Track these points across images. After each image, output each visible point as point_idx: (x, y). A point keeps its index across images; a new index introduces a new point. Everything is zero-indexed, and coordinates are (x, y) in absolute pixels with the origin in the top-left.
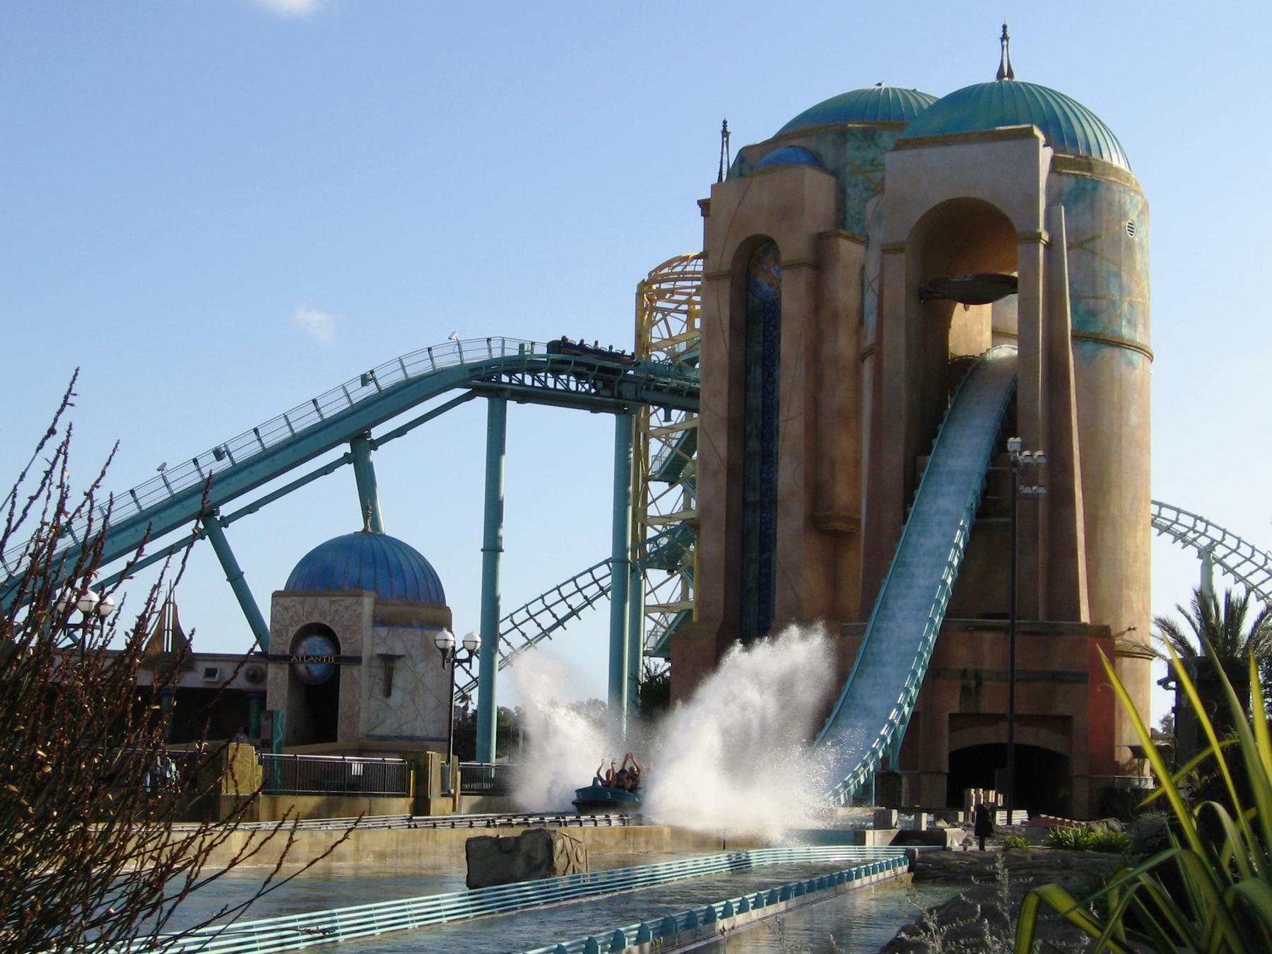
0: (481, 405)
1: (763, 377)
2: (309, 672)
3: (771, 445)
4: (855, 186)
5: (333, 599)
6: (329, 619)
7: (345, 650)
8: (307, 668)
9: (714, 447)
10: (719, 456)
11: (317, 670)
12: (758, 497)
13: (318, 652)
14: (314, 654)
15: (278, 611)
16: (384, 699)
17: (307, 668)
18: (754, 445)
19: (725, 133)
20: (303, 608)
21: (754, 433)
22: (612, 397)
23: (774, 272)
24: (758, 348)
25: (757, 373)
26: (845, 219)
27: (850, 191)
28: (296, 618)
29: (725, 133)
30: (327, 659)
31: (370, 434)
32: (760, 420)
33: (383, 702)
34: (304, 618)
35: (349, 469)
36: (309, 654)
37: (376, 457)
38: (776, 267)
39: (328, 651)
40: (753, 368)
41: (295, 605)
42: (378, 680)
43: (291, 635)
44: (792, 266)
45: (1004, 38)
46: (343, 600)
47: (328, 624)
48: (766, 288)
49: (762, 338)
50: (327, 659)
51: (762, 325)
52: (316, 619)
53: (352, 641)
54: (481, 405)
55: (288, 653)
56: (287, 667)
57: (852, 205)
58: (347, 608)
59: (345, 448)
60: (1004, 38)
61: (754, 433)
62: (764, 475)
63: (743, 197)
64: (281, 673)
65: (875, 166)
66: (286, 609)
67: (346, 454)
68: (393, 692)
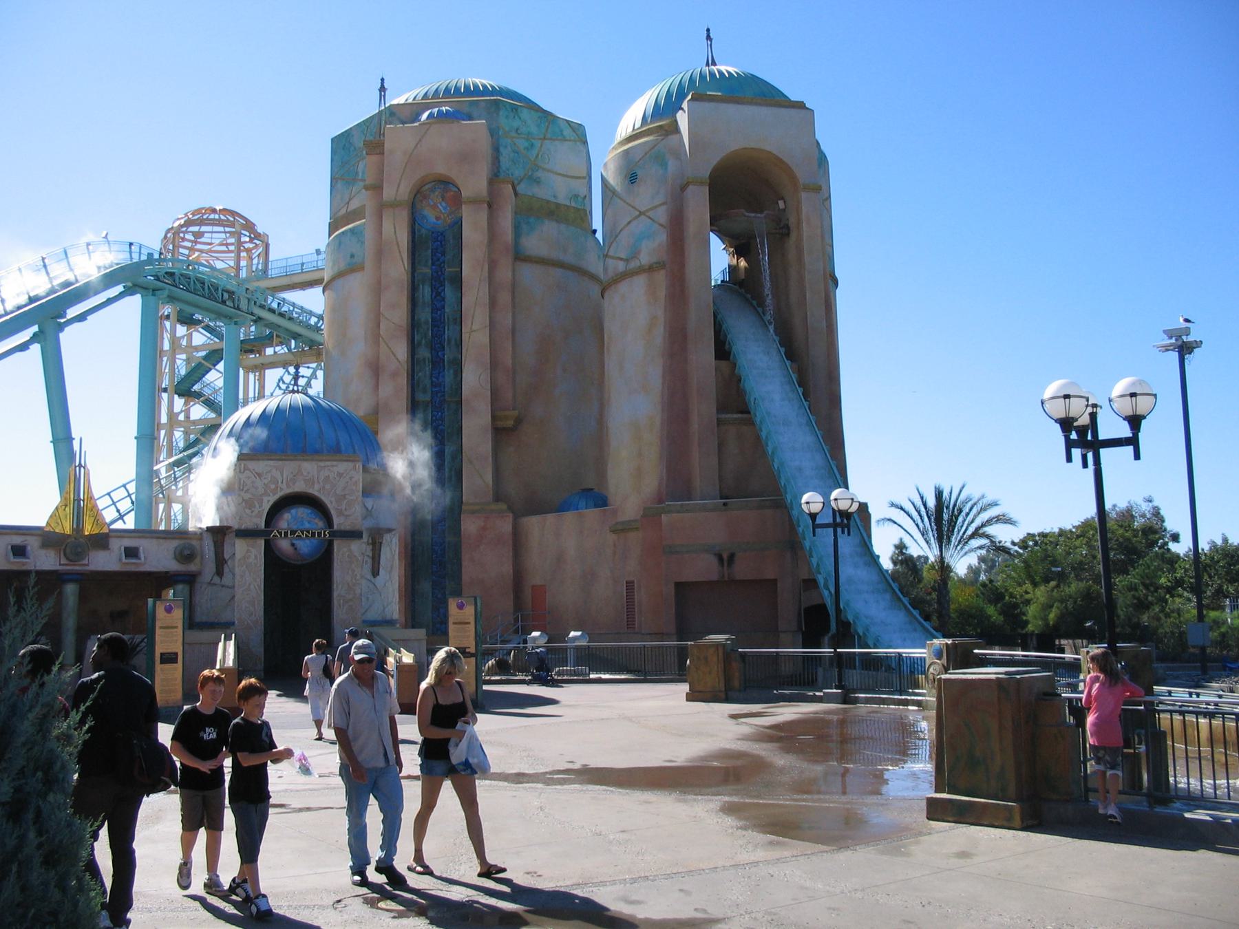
0: (135, 301)
1: (432, 295)
2: (296, 549)
3: (440, 354)
4: (506, 147)
5: (322, 464)
6: (317, 487)
7: (338, 523)
8: (293, 545)
9: (393, 353)
10: (397, 359)
11: (305, 546)
12: (428, 397)
13: (307, 526)
14: (301, 527)
15: (249, 478)
16: (373, 580)
17: (293, 545)
18: (424, 353)
19: (382, 89)
20: (282, 476)
21: (423, 342)
22: (234, 308)
23: (440, 207)
24: (426, 270)
25: (426, 292)
26: (499, 172)
27: (502, 149)
28: (273, 486)
29: (382, 89)
30: (319, 534)
31: (65, 312)
32: (430, 332)
33: (370, 581)
34: (284, 486)
35: (36, 349)
36: (295, 528)
37: (70, 338)
38: (444, 204)
39: (319, 524)
40: (421, 286)
41: (270, 471)
42: (366, 559)
43: (266, 507)
44: (474, 201)
45: (709, 37)
46: (336, 466)
47: (316, 493)
48: (432, 219)
49: (430, 262)
50: (319, 534)
51: (430, 251)
52: (299, 487)
53: (346, 513)
54: (135, 301)
55: (263, 526)
56: (262, 542)
57: (505, 162)
58: (340, 475)
59: (35, 328)
60: (709, 37)
61: (423, 342)
62: (434, 379)
63: (420, 140)
64: (254, 551)
65: (518, 134)
66: (260, 475)
67: (35, 334)
68: (382, 571)
